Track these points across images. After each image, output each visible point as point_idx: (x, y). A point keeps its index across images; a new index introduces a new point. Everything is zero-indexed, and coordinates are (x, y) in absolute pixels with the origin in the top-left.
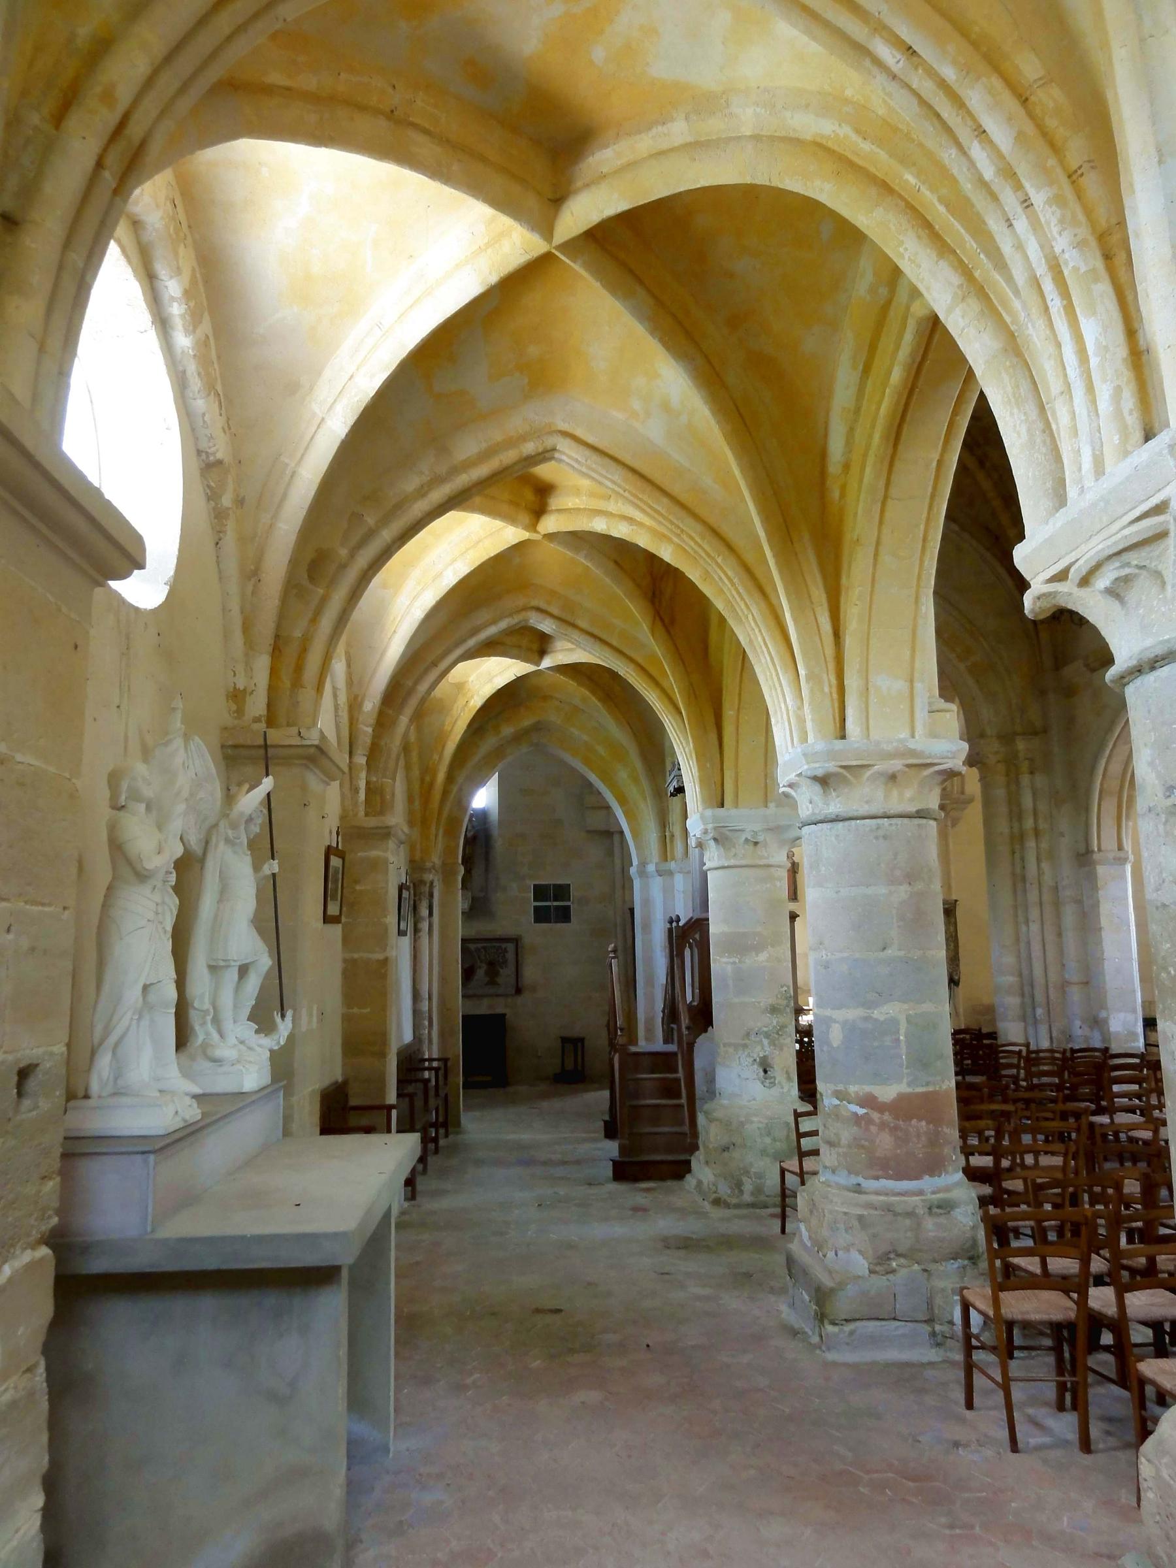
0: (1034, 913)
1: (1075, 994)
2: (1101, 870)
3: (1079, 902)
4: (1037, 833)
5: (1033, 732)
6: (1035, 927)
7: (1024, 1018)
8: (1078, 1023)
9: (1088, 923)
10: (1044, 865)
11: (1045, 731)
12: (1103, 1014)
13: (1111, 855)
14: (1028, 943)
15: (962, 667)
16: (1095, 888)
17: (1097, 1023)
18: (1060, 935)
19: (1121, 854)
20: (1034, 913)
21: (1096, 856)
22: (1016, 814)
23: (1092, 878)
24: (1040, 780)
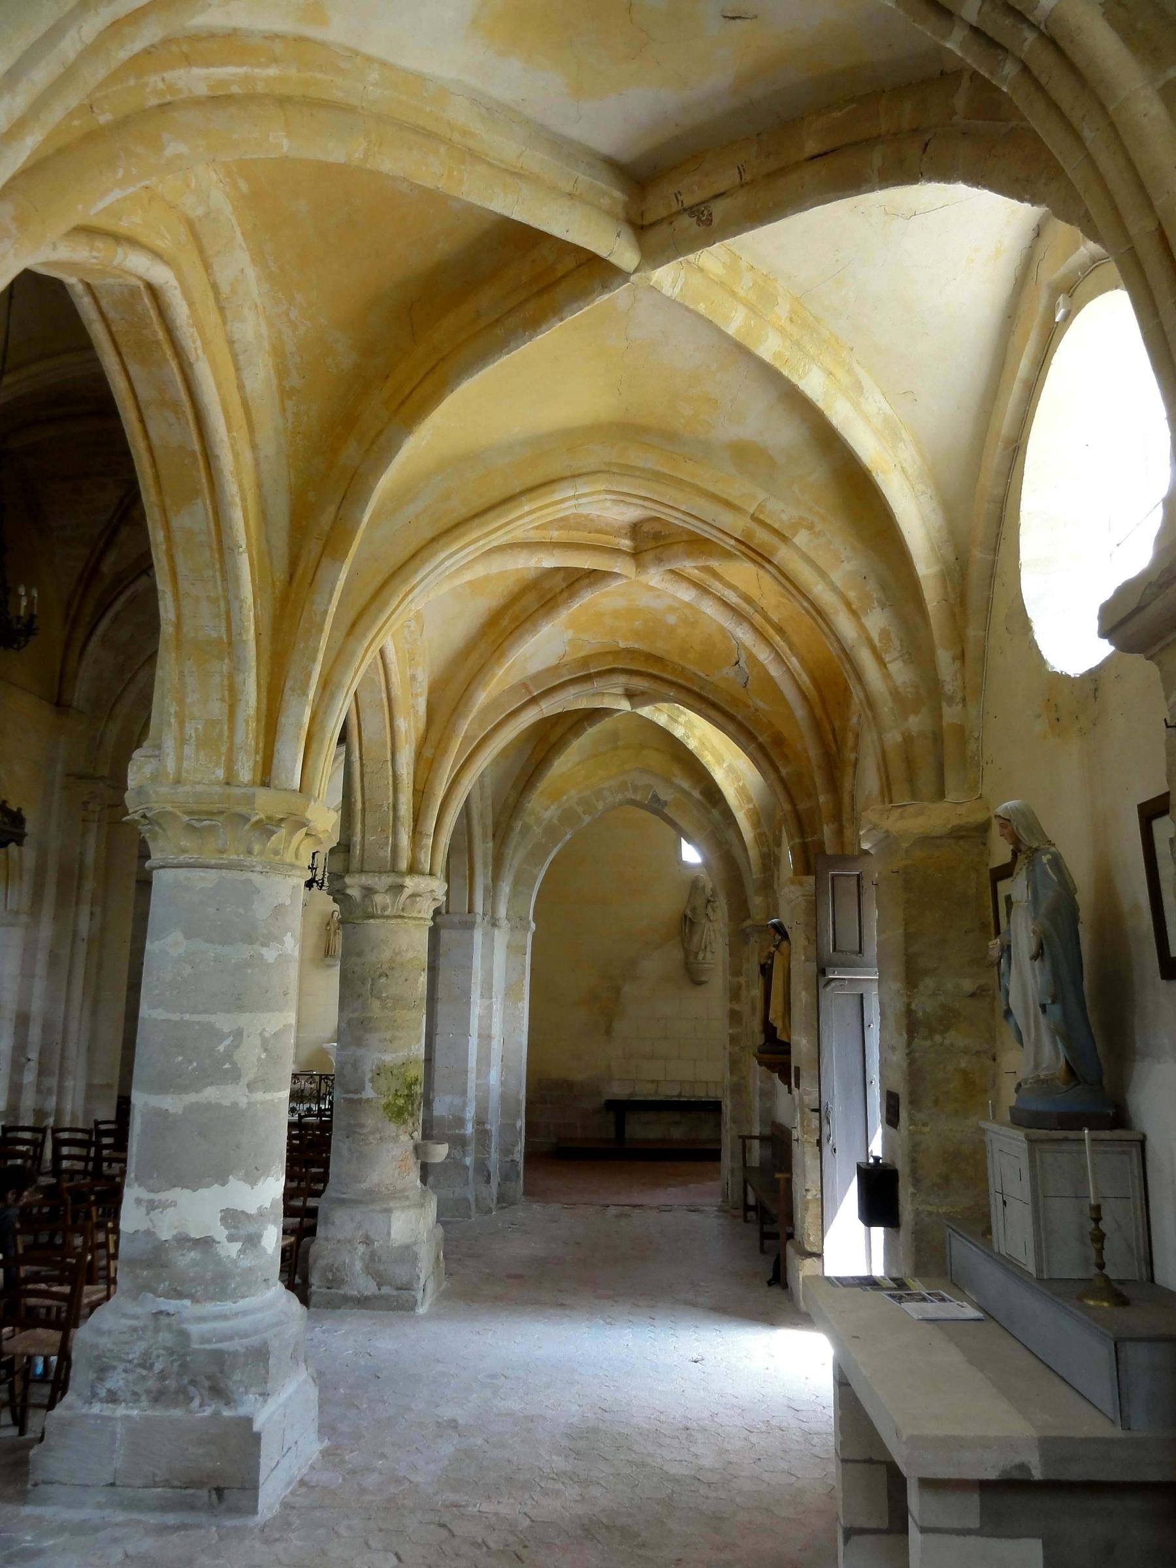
19: (469, 918)
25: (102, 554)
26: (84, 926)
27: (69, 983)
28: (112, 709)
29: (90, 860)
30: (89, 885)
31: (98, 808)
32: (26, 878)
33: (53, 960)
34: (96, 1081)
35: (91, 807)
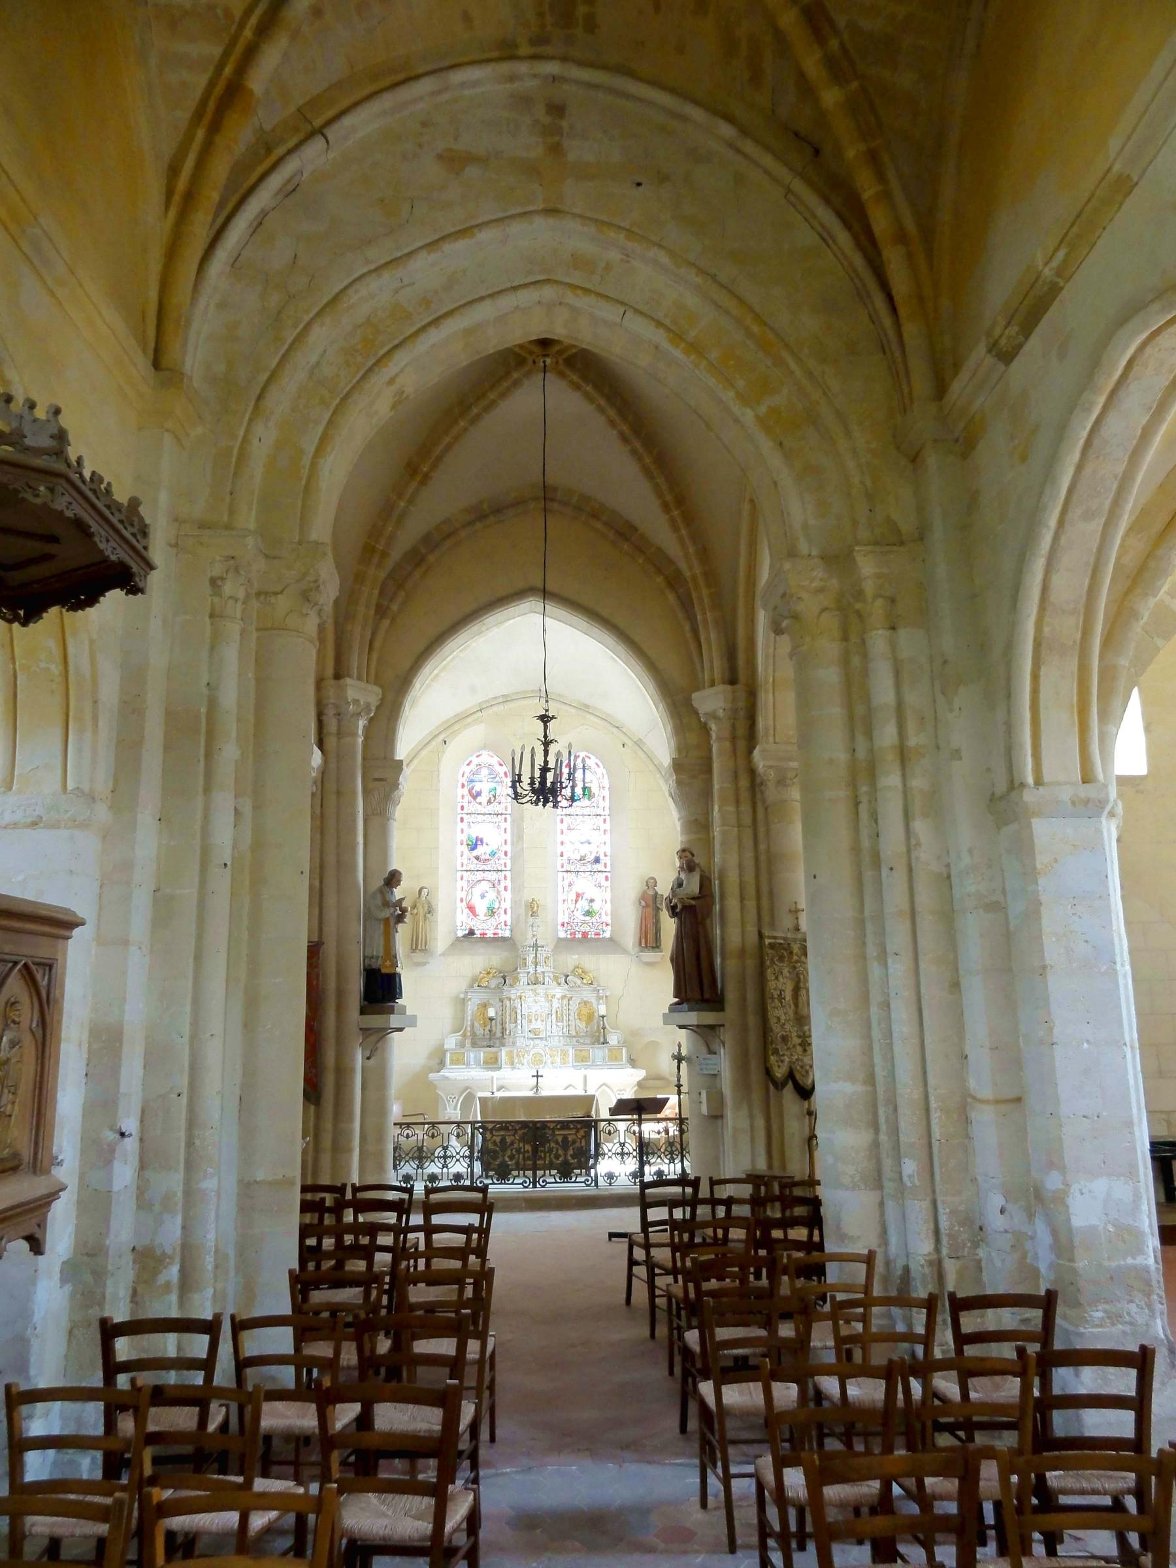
0: (898, 936)
1: (987, 1126)
2: (1045, 832)
3: (996, 907)
4: (903, 755)
5: (891, 539)
6: (899, 969)
7: (876, 1181)
8: (996, 1200)
9: (1015, 962)
10: (920, 827)
11: (921, 535)
12: (1053, 1182)
13: (1065, 794)
14: (886, 1005)
15: (748, 416)
16: (1030, 874)
17: (1037, 1200)
18: (955, 986)
20: (898, 936)
21: (1029, 796)
22: (860, 721)
23: (1023, 847)
24: (910, 641)
25: (250, 54)
26: (224, 836)
27: (198, 957)
28: (260, 397)
29: (229, 697)
30: (229, 752)
31: (241, 594)
32: (105, 722)
33: (163, 908)
34: (260, 1176)
35: (228, 588)
